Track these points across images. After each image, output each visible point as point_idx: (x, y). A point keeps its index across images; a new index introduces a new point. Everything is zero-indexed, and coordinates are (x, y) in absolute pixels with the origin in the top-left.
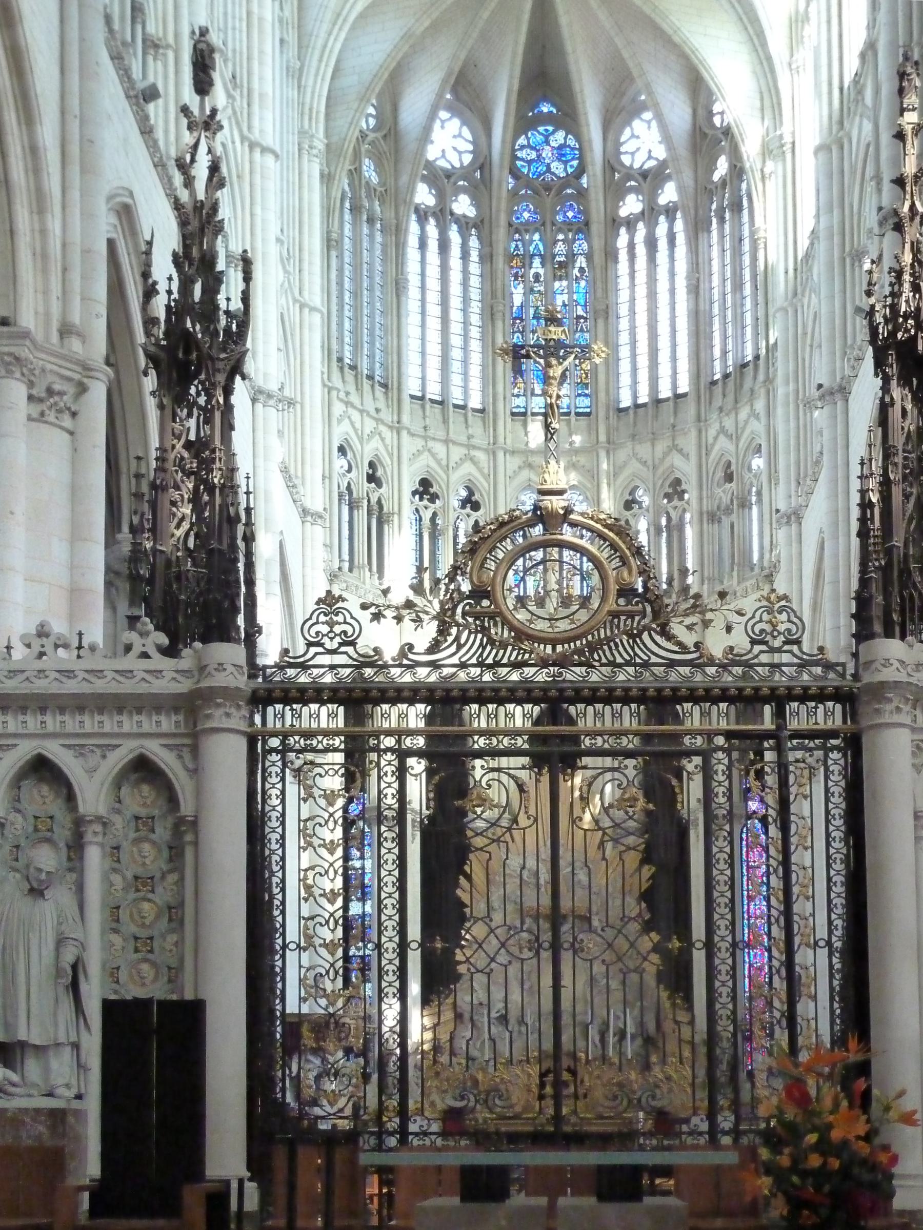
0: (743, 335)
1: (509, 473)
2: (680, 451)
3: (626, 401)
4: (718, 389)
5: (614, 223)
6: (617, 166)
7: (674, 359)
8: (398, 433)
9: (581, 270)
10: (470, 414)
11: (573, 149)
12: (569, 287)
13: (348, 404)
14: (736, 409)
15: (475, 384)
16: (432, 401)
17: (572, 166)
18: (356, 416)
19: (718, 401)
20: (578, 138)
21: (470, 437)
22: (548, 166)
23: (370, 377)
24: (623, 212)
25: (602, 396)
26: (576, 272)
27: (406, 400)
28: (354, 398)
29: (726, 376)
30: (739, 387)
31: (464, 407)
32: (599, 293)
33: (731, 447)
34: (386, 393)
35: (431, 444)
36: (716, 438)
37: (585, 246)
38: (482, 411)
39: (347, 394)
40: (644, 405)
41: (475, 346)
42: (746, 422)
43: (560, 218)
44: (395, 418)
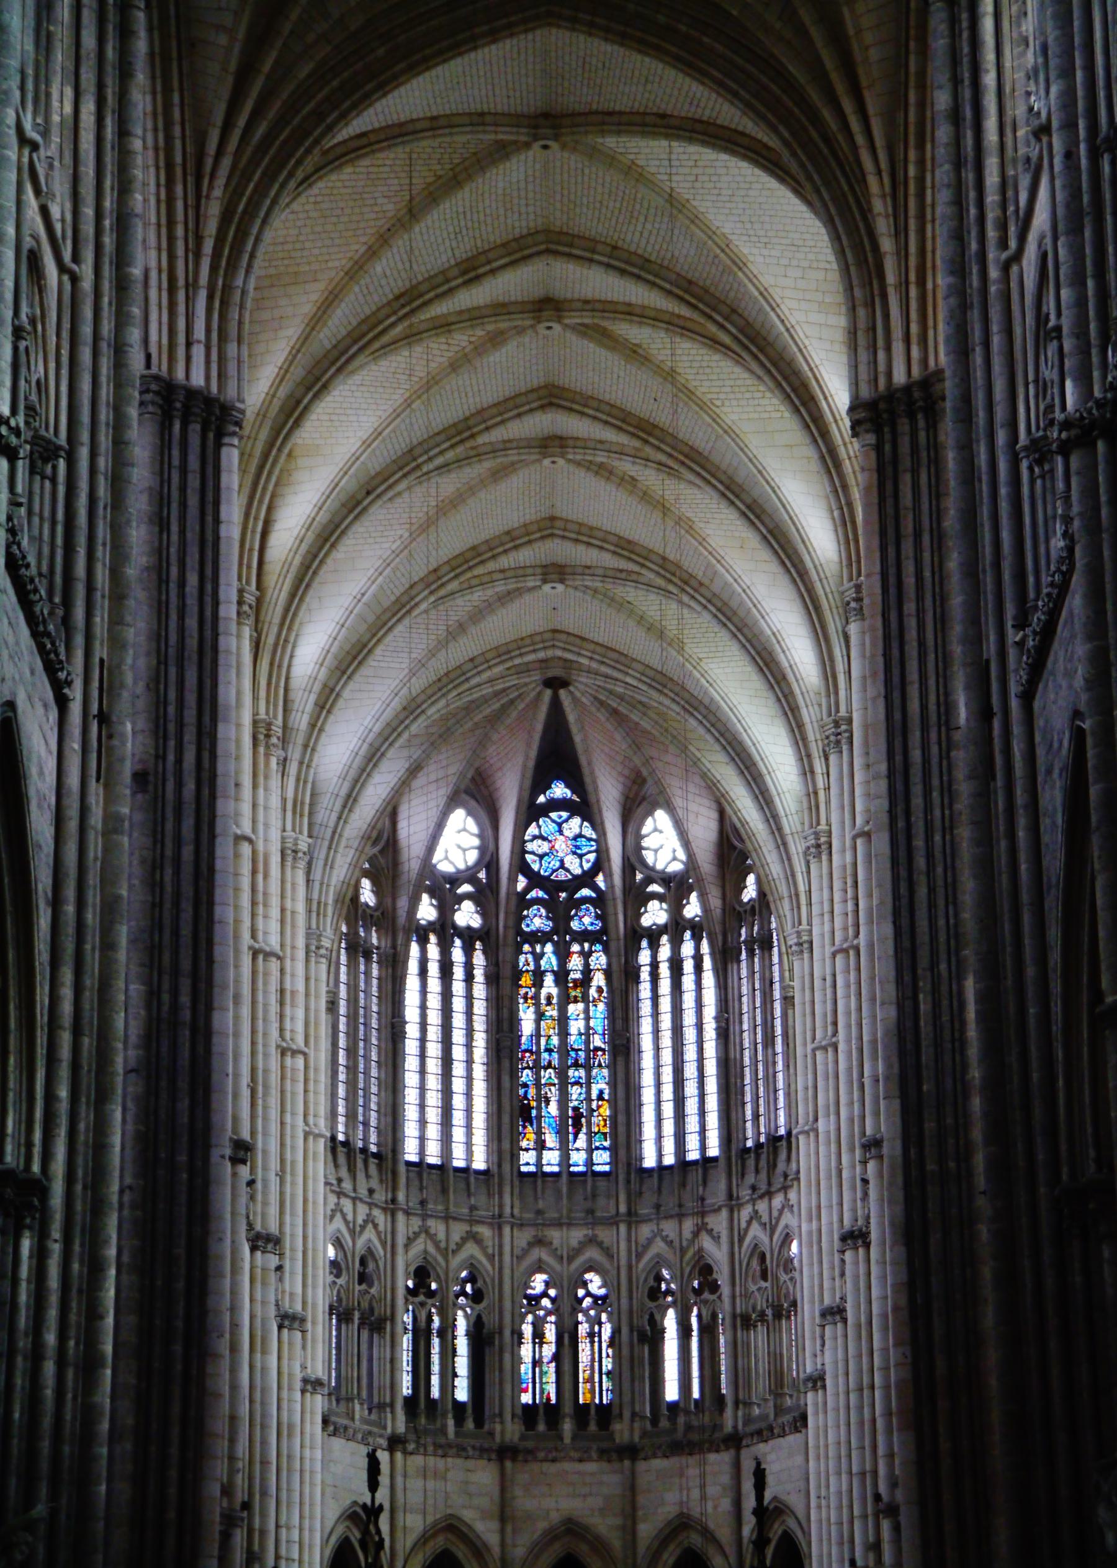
0: (776, 1099)
1: (517, 1252)
2: (710, 1232)
3: (650, 1162)
4: (751, 1162)
5: (636, 935)
6: (637, 865)
7: (702, 1113)
8: (393, 1215)
9: (600, 990)
10: (472, 1179)
11: (590, 840)
12: (587, 1011)
13: (340, 1194)
14: (769, 1194)
15: (480, 1138)
16: (431, 1167)
17: (588, 861)
18: (347, 1206)
19: (750, 1179)
20: (594, 828)
21: (473, 1208)
22: (562, 862)
23: (364, 1150)
24: (646, 921)
25: (622, 1153)
26: (593, 992)
27: (402, 1169)
28: (347, 1185)
29: (758, 1146)
30: (772, 1166)
31: (466, 1170)
32: (619, 1024)
33: (764, 1238)
34: (380, 1167)
35: (431, 1223)
36: (749, 1223)
37: (603, 960)
38: (485, 1173)
39: (340, 1180)
40: (670, 1167)
41: (480, 1088)
42: (781, 1212)
43: (575, 925)
44: (390, 1196)
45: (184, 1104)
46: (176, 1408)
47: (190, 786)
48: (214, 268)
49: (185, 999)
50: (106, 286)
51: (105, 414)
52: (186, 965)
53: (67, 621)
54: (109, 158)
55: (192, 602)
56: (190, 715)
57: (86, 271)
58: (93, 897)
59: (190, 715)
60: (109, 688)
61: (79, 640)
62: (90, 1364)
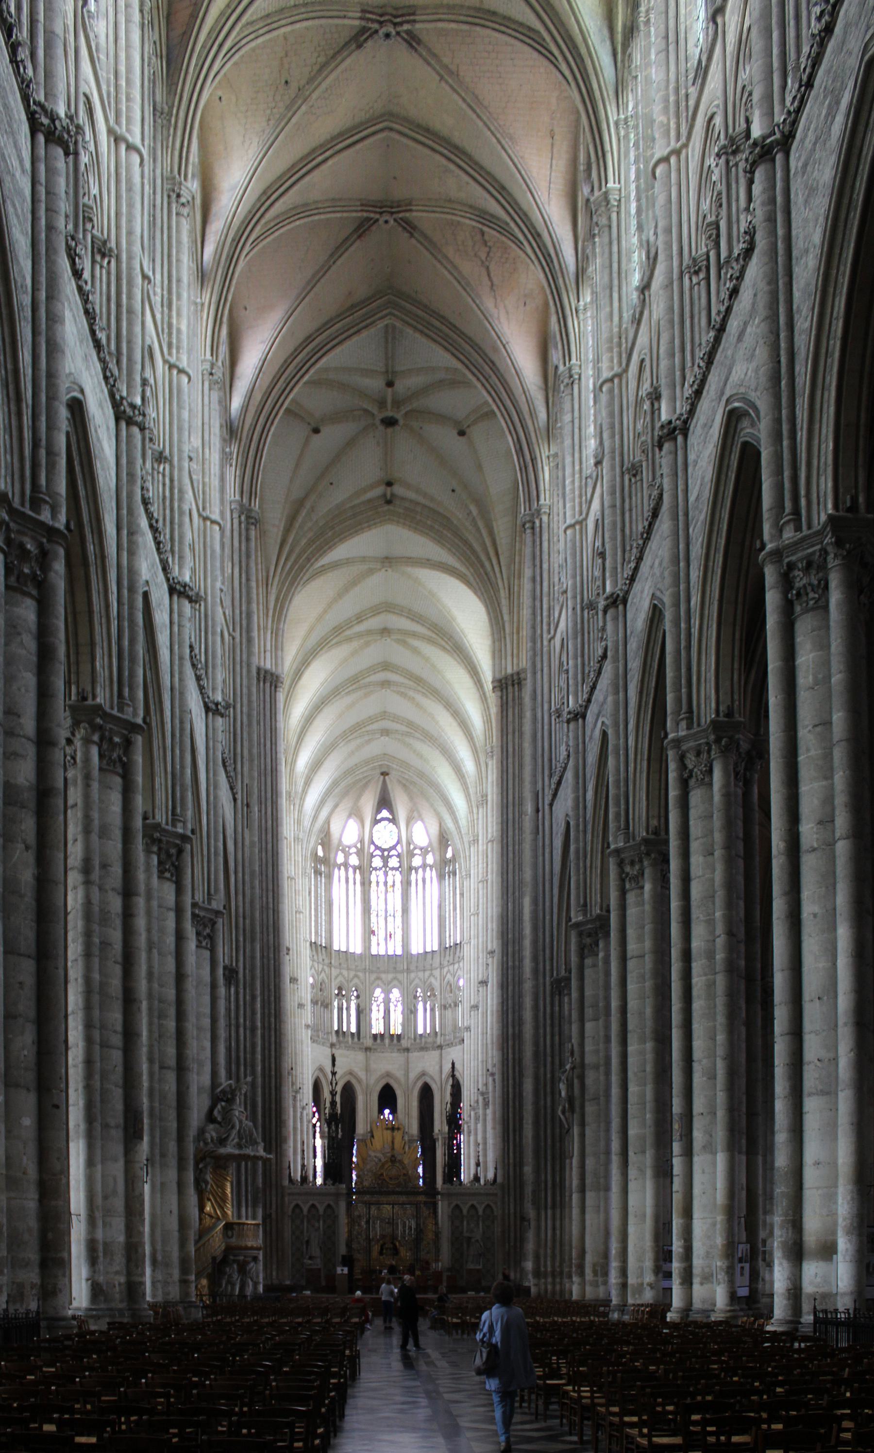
45: (271, 937)
46: (273, 1039)
47: (270, 822)
48: (273, 621)
49: (271, 900)
50: (244, 640)
51: (245, 690)
52: (270, 887)
53: (235, 769)
54: (244, 590)
55: (268, 752)
56: (269, 795)
57: (237, 635)
58: (247, 871)
59: (269, 795)
60: (249, 794)
61: (239, 777)
62: (253, 1029)
